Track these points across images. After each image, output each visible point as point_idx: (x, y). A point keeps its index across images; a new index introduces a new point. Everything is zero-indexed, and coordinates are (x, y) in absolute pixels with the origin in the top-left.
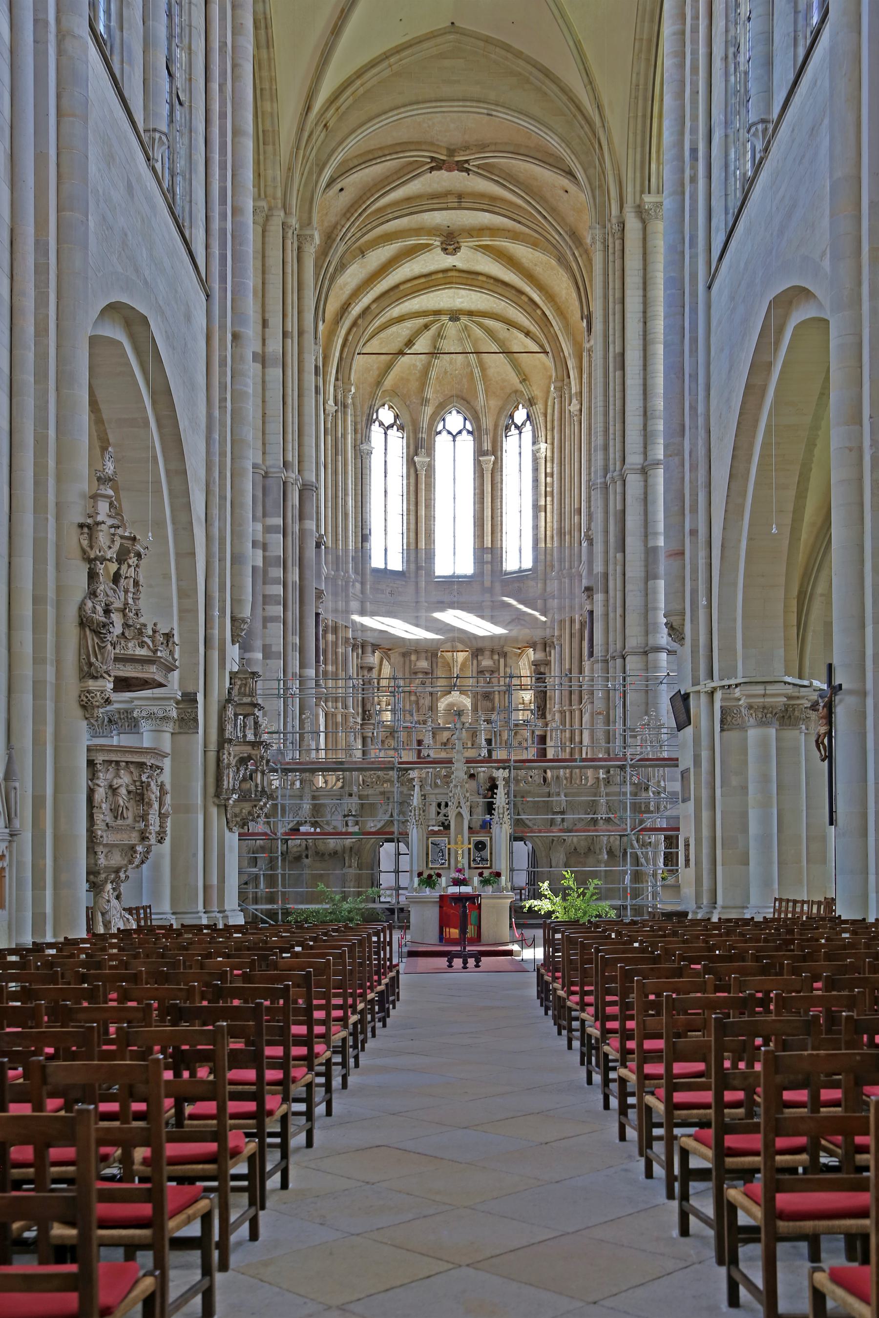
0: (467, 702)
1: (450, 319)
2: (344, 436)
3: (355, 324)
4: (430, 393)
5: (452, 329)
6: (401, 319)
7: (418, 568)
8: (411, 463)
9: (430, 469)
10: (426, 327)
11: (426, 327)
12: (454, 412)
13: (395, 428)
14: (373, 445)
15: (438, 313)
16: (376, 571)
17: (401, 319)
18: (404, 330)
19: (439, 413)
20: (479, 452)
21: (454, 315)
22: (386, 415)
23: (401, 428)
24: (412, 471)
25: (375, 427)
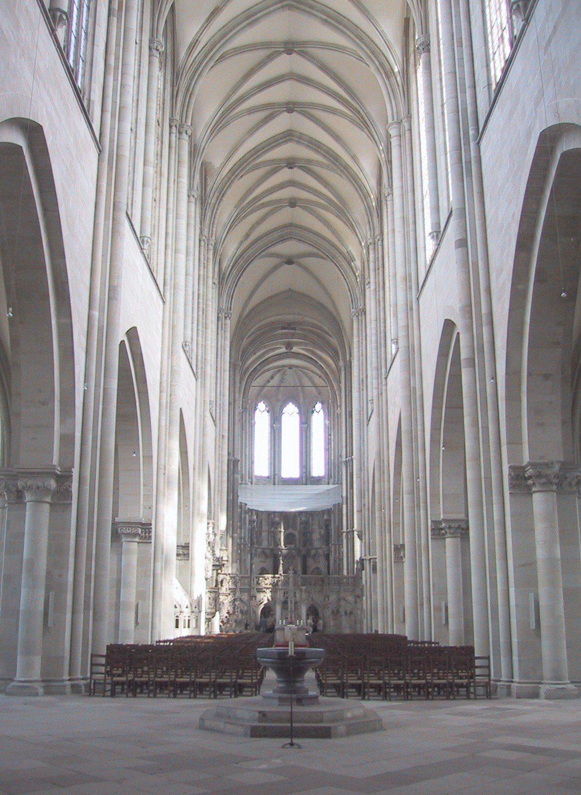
1: (289, 368)
2: (245, 421)
3: (250, 374)
4: (280, 397)
5: (288, 371)
6: (268, 370)
11: (279, 371)
12: (290, 404)
13: (266, 411)
14: (256, 421)
15: (284, 366)
18: (269, 374)
20: (301, 423)
21: (290, 367)
23: (268, 411)
24: (273, 433)
25: (257, 413)
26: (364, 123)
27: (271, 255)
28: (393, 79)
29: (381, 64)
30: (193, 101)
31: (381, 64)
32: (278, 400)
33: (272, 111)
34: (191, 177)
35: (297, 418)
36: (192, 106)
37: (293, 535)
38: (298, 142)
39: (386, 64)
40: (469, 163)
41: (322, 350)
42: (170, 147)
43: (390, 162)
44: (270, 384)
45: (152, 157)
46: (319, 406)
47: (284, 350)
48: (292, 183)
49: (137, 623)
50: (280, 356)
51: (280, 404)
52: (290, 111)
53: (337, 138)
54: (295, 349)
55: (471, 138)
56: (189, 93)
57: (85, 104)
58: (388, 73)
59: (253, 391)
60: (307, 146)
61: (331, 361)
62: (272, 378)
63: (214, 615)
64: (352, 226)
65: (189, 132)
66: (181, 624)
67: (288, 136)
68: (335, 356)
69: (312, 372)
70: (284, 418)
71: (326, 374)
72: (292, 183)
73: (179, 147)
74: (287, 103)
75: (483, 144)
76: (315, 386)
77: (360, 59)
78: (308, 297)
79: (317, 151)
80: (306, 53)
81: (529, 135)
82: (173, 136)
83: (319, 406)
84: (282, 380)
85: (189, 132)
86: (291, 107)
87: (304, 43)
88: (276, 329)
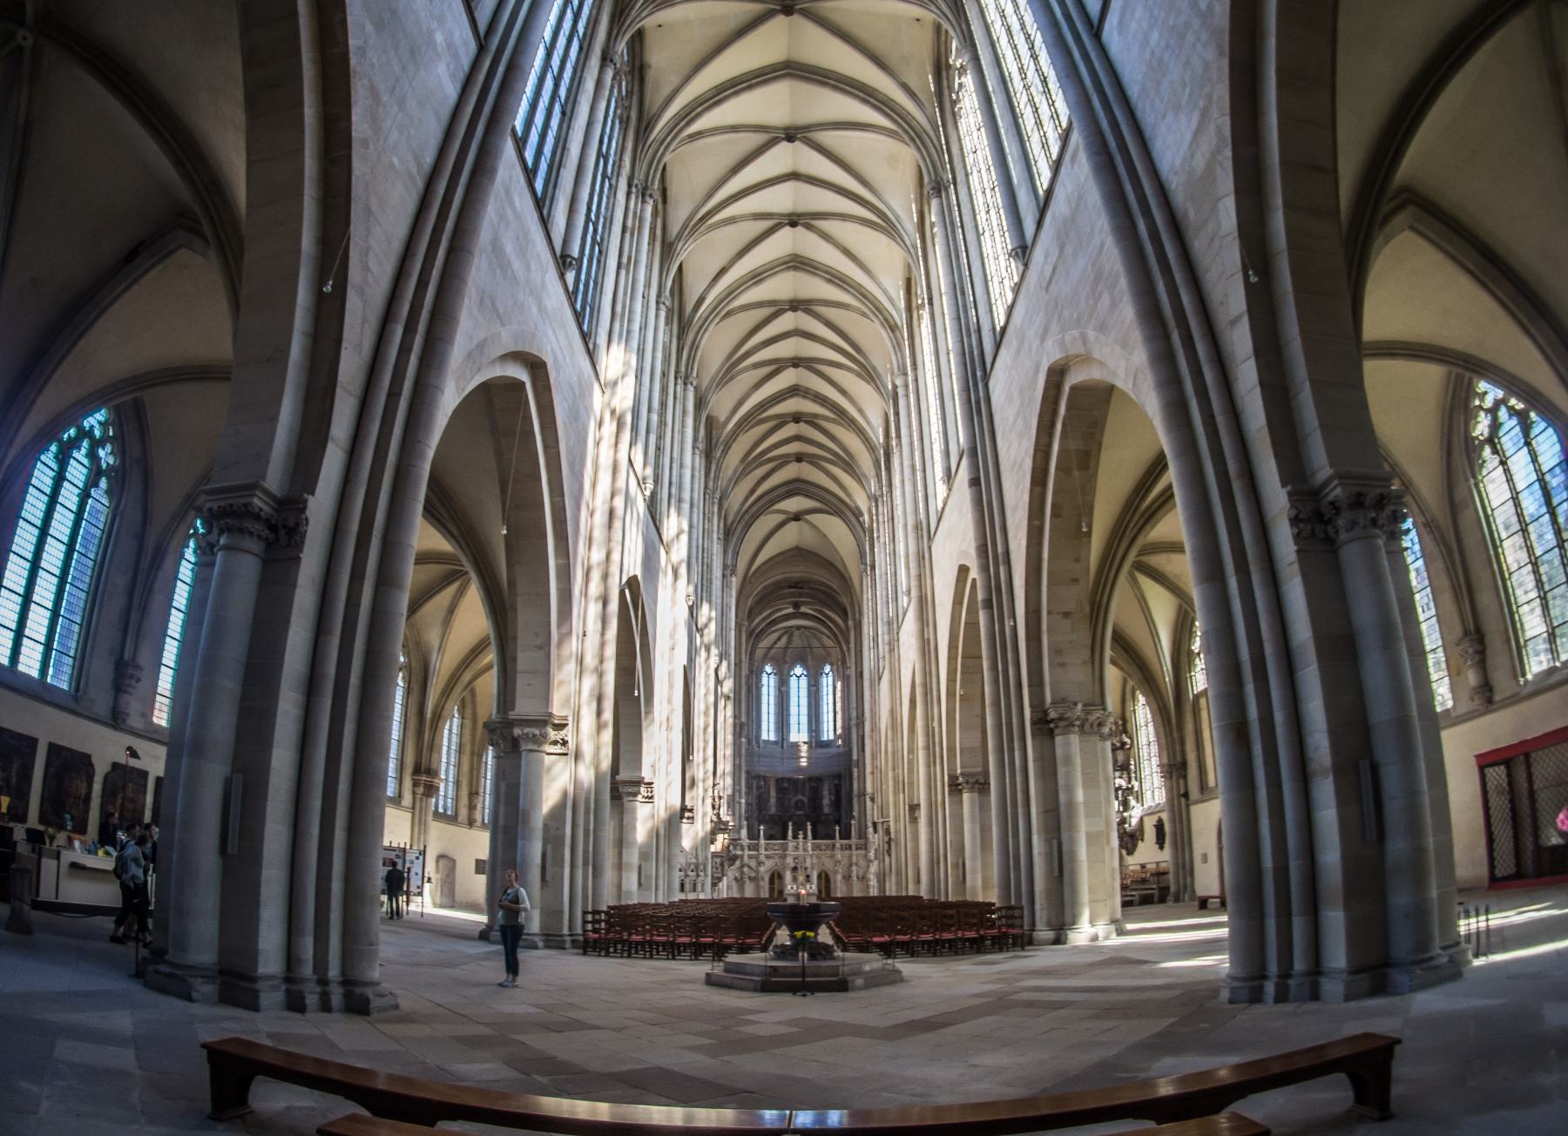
0: (806, 800)
4: (788, 659)
5: (796, 633)
6: (776, 630)
7: (783, 739)
8: (780, 691)
9: (788, 693)
10: (786, 632)
11: (786, 632)
15: (791, 627)
16: (765, 741)
17: (776, 630)
18: (776, 635)
19: (792, 667)
20: (810, 686)
21: (798, 628)
22: (768, 669)
23: (775, 674)
25: (764, 675)
26: (869, 374)
27: (779, 512)
28: (898, 333)
29: (886, 320)
30: (699, 354)
31: (886, 320)
32: (786, 662)
33: (779, 366)
34: (696, 430)
35: (804, 682)
36: (697, 359)
37: (802, 802)
38: (805, 397)
39: (890, 318)
40: (978, 402)
41: (831, 609)
42: (675, 398)
43: (897, 414)
44: (777, 646)
45: (656, 404)
46: (827, 669)
47: (790, 610)
48: (797, 438)
49: (640, 884)
50: (788, 617)
51: (787, 666)
52: (796, 365)
53: (843, 392)
54: (803, 609)
55: (979, 379)
56: (694, 346)
57: (591, 346)
58: (893, 328)
59: (759, 653)
60: (814, 401)
61: (840, 622)
62: (779, 639)
63: (720, 879)
64: (860, 479)
65: (695, 383)
66: (687, 887)
67: (795, 391)
68: (844, 613)
69: (822, 633)
70: (793, 681)
71: (834, 634)
72: (797, 438)
73: (685, 398)
74: (794, 359)
75: (991, 384)
76: (824, 647)
77: (864, 315)
78: (816, 554)
79: (823, 405)
80: (811, 311)
81: (1037, 371)
82: (679, 388)
83: (827, 669)
84: (790, 641)
85: (695, 383)
86: (796, 362)
87: (811, 302)
88: (782, 588)
